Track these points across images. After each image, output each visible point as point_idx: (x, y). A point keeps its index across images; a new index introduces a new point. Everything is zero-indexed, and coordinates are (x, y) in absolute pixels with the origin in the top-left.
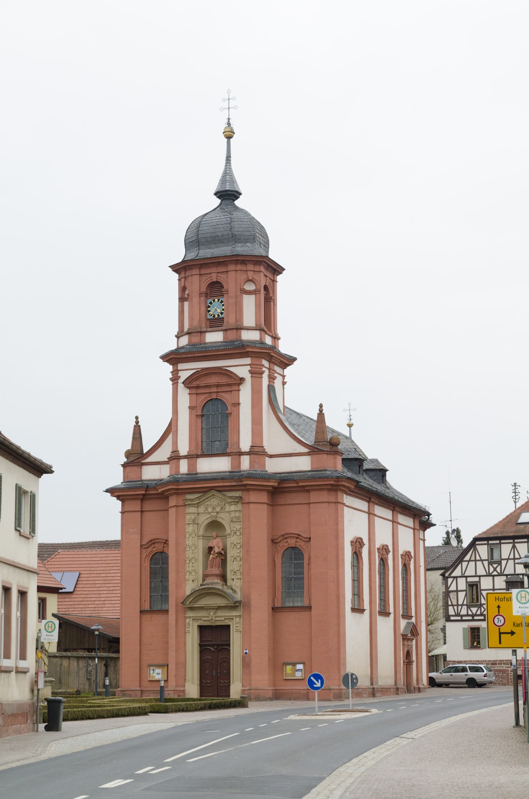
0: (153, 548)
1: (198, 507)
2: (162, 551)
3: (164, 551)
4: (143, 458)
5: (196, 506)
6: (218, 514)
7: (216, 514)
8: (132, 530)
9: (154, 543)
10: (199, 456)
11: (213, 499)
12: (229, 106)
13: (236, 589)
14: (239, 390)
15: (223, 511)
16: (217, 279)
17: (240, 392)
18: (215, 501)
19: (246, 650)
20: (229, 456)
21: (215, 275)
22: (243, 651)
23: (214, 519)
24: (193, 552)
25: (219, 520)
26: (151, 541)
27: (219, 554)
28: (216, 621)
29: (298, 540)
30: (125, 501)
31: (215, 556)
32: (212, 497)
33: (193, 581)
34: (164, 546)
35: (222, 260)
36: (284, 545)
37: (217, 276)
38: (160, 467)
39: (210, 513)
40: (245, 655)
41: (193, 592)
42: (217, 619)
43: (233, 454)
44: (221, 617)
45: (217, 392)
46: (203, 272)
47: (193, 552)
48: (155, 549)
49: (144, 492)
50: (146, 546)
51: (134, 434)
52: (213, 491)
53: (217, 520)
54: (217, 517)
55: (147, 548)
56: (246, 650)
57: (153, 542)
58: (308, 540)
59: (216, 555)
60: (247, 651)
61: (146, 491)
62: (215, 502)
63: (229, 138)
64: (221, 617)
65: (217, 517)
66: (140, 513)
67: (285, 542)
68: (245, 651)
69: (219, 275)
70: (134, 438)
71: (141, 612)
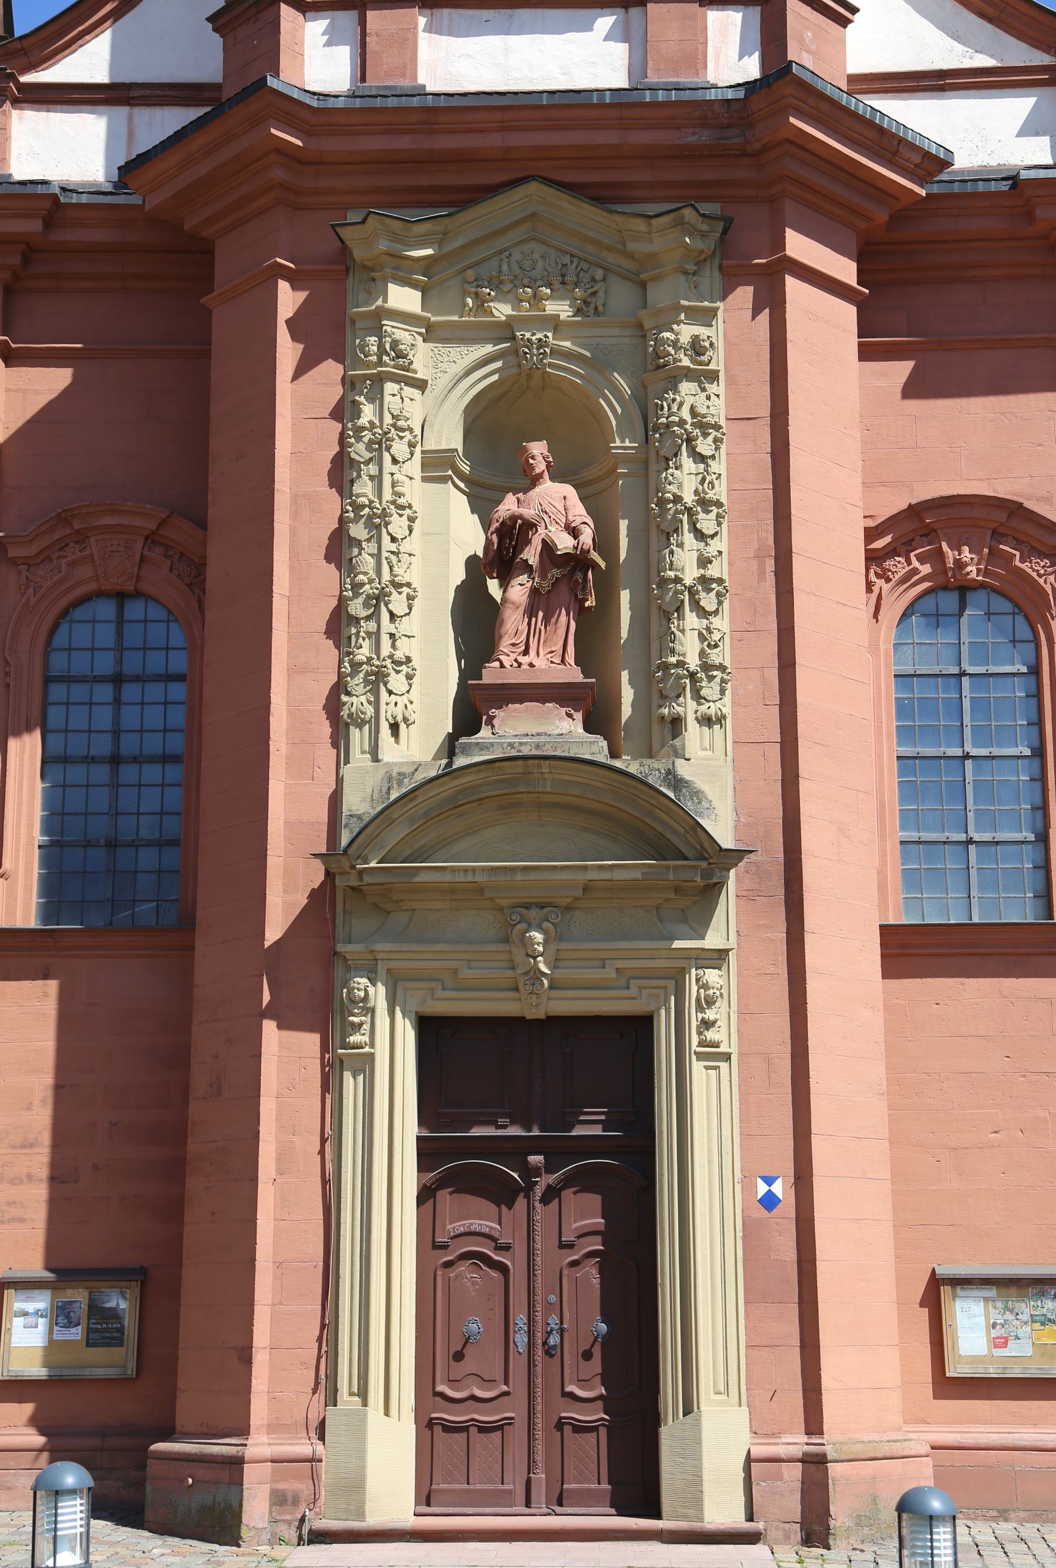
0: (72, 564)
2: (129, 587)
9: (81, 538)
11: (527, 248)
13: (699, 783)
18: (536, 256)
19: (769, 1181)
22: (748, 1188)
24: (393, 547)
26: (63, 519)
33: (395, 728)
34: (142, 559)
36: (915, 571)
38: (130, 118)
40: (761, 1212)
41: (394, 795)
47: (393, 547)
48: (85, 571)
52: (533, 188)
56: (769, 1181)
57: (77, 525)
59: (556, 573)
60: (777, 1188)
68: (762, 1188)
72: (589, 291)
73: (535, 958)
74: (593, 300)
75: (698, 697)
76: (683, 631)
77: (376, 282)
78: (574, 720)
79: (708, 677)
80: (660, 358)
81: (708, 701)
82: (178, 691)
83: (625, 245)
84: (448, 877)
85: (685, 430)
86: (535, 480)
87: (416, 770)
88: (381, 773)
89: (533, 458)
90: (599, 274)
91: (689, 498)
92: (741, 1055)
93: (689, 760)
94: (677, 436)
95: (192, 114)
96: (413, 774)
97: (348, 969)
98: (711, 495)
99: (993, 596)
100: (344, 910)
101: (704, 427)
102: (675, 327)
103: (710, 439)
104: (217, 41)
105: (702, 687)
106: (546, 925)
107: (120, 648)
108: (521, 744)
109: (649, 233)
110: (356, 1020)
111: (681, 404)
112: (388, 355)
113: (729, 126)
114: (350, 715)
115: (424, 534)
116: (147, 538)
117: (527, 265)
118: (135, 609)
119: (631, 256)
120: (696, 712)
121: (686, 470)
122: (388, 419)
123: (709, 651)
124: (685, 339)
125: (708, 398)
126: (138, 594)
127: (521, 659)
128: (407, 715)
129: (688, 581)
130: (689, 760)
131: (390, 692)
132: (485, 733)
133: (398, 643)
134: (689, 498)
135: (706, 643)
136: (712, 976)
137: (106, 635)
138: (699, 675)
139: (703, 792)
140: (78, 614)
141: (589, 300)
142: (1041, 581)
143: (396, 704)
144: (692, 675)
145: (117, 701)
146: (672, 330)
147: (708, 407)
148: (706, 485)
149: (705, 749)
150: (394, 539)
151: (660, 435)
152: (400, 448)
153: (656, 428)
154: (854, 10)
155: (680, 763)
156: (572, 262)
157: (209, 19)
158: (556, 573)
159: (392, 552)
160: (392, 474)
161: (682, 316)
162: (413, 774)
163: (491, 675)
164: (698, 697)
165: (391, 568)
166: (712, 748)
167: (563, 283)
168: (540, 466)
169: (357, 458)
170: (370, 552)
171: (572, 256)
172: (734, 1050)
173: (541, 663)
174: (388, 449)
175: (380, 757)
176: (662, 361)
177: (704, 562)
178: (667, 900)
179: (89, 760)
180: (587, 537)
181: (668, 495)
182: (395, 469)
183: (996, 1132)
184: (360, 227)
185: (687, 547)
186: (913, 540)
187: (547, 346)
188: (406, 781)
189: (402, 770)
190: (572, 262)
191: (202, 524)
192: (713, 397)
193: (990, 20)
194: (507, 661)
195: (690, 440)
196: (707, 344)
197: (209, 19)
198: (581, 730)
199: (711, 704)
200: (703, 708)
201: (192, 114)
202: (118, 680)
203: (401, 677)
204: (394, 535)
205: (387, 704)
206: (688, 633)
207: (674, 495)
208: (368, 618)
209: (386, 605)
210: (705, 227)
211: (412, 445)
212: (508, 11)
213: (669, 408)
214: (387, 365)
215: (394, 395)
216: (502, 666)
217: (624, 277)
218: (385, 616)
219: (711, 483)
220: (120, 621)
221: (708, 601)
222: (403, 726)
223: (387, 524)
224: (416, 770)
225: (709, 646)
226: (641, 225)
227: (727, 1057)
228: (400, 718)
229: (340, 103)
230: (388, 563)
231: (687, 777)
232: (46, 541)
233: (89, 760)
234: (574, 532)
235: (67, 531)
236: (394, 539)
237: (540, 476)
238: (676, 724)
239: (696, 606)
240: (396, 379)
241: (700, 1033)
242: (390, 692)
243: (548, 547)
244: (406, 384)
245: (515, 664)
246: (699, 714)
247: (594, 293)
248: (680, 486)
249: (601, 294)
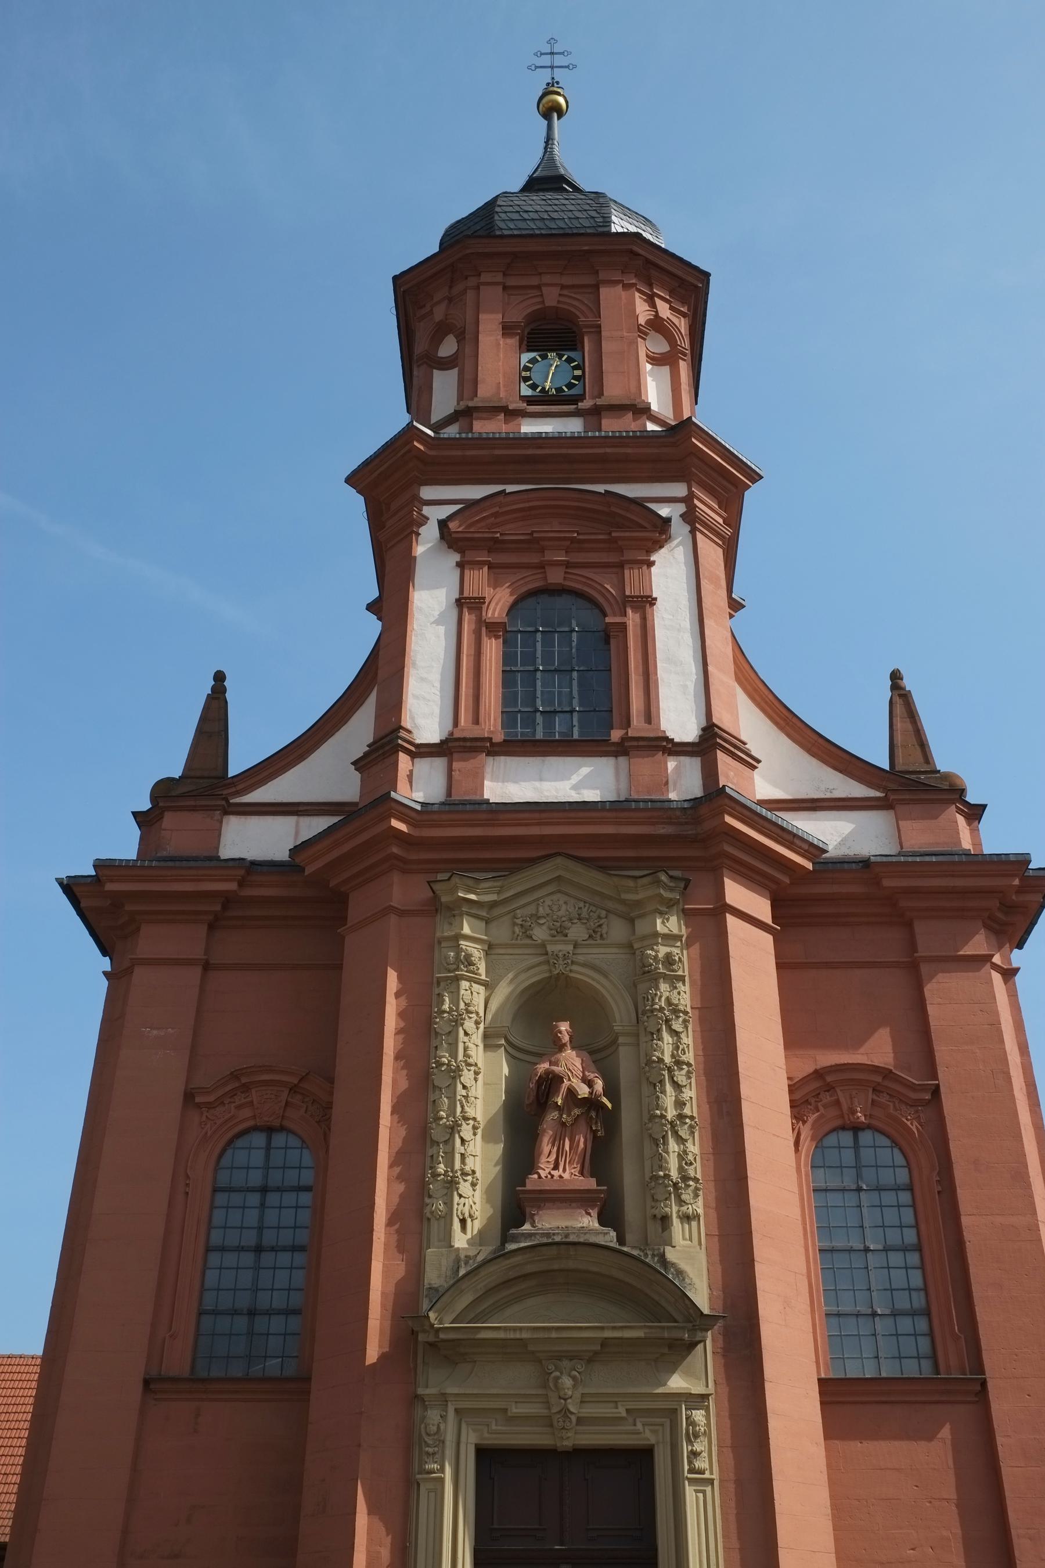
0: (239, 1107)
1: (487, 922)
2: (276, 1123)
3: (286, 1123)
4: (233, 790)
5: (484, 914)
6: (579, 951)
7: (570, 948)
8: (155, 1032)
9: (246, 1088)
10: (496, 749)
11: (555, 897)
12: (556, 53)
13: (683, 1265)
14: (651, 564)
15: (599, 942)
16: (559, 302)
17: (654, 570)
18: (561, 902)
20: (616, 754)
21: (556, 291)
23: (560, 968)
24: (464, 1093)
25: (580, 973)
26: (235, 1076)
27: (589, 1110)
28: (580, 1421)
29: (883, 1099)
30: (138, 929)
31: (569, 1115)
32: (550, 889)
33: (463, 1222)
34: (287, 1103)
35: (586, 248)
37: (560, 295)
38: (297, 824)
39: (543, 945)
41: (462, 1272)
42: (588, 1411)
43: (641, 743)
44: (613, 1399)
45: (568, 565)
46: (512, 282)
47: (464, 1093)
48: (247, 1113)
49: (233, 886)
50: (211, 1098)
51: (204, 719)
52: (559, 860)
53: (572, 975)
54: (573, 962)
55: (209, 1106)
57: (244, 1080)
58: (928, 1097)
61: (241, 884)
62: (564, 907)
63: (550, 111)
64: (613, 1399)
65: (573, 962)
66: (199, 970)
67: (825, 1101)
69: (565, 292)
70: (200, 732)
71: (147, 1382)
72: (597, 924)
73: (565, 1400)
74: (600, 930)
75: (681, 1202)
76: (667, 1153)
77: (456, 918)
78: (591, 1216)
79: (685, 1185)
80: (645, 967)
81: (688, 1204)
82: (305, 1198)
83: (620, 896)
84: (501, 1335)
85: (665, 1014)
86: (561, 1047)
87: (478, 1253)
88: (453, 1256)
89: (560, 1032)
90: (603, 913)
91: (668, 1059)
92: (721, 1481)
93: (674, 1247)
94: (659, 1018)
95: (335, 819)
96: (476, 1256)
97: (426, 1409)
98: (684, 1058)
99: (877, 1135)
100: (423, 1361)
101: (676, 1011)
102: (655, 947)
103: (681, 1019)
104: (357, 776)
105: (682, 1193)
106: (574, 1373)
107: (267, 1167)
108: (554, 1234)
109: (636, 887)
110: (430, 1450)
111: (661, 997)
112: (463, 964)
113: (686, 823)
114: (432, 1213)
115: (485, 1084)
116: (291, 1089)
117: (555, 908)
118: (279, 1139)
119: (623, 902)
120: (679, 1211)
121: (666, 1042)
122: (462, 1006)
123: (686, 1167)
124: (661, 955)
125: (679, 993)
126: (282, 1129)
127: (553, 1172)
128: (472, 1213)
129: (669, 1118)
130: (674, 1247)
131: (460, 1196)
132: (527, 1227)
133: (467, 1160)
135: (684, 1162)
136: (699, 1415)
137: (257, 1158)
138: (680, 1185)
139: (686, 1272)
140: (240, 1143)
141: (597, 930)
142: (909, 1123)
143: (464, 1204)
144: (675, 1185)
145: (263, 1205)
146: (652, 949)
147: (679, 999)
148: (680, 1052)
149: (686, 1240)
150: (464, 1087)
151: (648, 1017)
153: (644, 1013)
154: (758, 761)
155: (668, 1249)
156: (585, 906)
157: (352, 763)
158: (576, 1112)
159: (463, 1096)
160: (464, 1043)
161: (660, 940)
162: (476, 1256)
163: (532, 1182)
164: (681, 1202)
165: (462, 1107)
166: (691, 1239)
167: (579, 919)
168: (566, 1038)
169: (441, 1032)
170: (448, 1095)
171: (585, 902)
172: (715, 1476)
173: (566, 1176)
174: (462, 1025)
175: (452, 1244)
176: (647, 969)
177: (680, 1104)
178: (663, 1354)
179: (240, 1249)
180: (599, 1085)
181: (654, 1058)
182: (466, 1039)
183: (913, 1549)
184: (447, 882)
185: (668, 1094)
186: (819, 1094)
187: (569, 959)
188: (471, 1261)
189: (468, 1254)
190: (585, 906)
191: (331, 1080)
192: (682, 993)
193: (841, 772)
194: (543, 1174)
195: (667, 1021)
196: (677, 958)
197: (352, 763)
198: (597, 1225)
199: (690, 1206)
200: (684, 1209)
201: (335, 819)
202: (264, 1190)
203: (468, 1184)
204: (465, 1084)
205: (458, 1204)
206: (671, 1154)
207: (658, 1057)
208: (446, 1142)
209: (459, 1132)
210: (672, 884)
211: (477, 1023)
212: (542, 758)
213: (653, 1000)
214: (462, 971)
215: (466, 990)
216: (540, 1177)
217: (619, 916)
218: (458, 1141)
219: (683, 1050)
220: (268, 1148)
221: (683, 1132)
222: (469, 1221)
223: (460, 1076)
224: (478, 1253)
225: (686, 1164)
226: (631, 883)
227: (711, 1482)
228: (467, 1215)
229: (436, 808)
230: (460, 1103)
231: (674, 1261)
232: (220, 1092)
233: (240, 1249)
234: (590, 1084)
235: (237, 1085)
236: (464, 1087)
237: (565, 1045)
238: (665, 1220)
239: (676, 1134)
240: (469, 980)
241: (690, 1462)
242: (460, 1196)
243: (571, 1092)
244: (475, 983)
245: (549, 1176)
246: (680, 1213)
247: (600, 926)
248: (663, 1053)
249: (605, 926)
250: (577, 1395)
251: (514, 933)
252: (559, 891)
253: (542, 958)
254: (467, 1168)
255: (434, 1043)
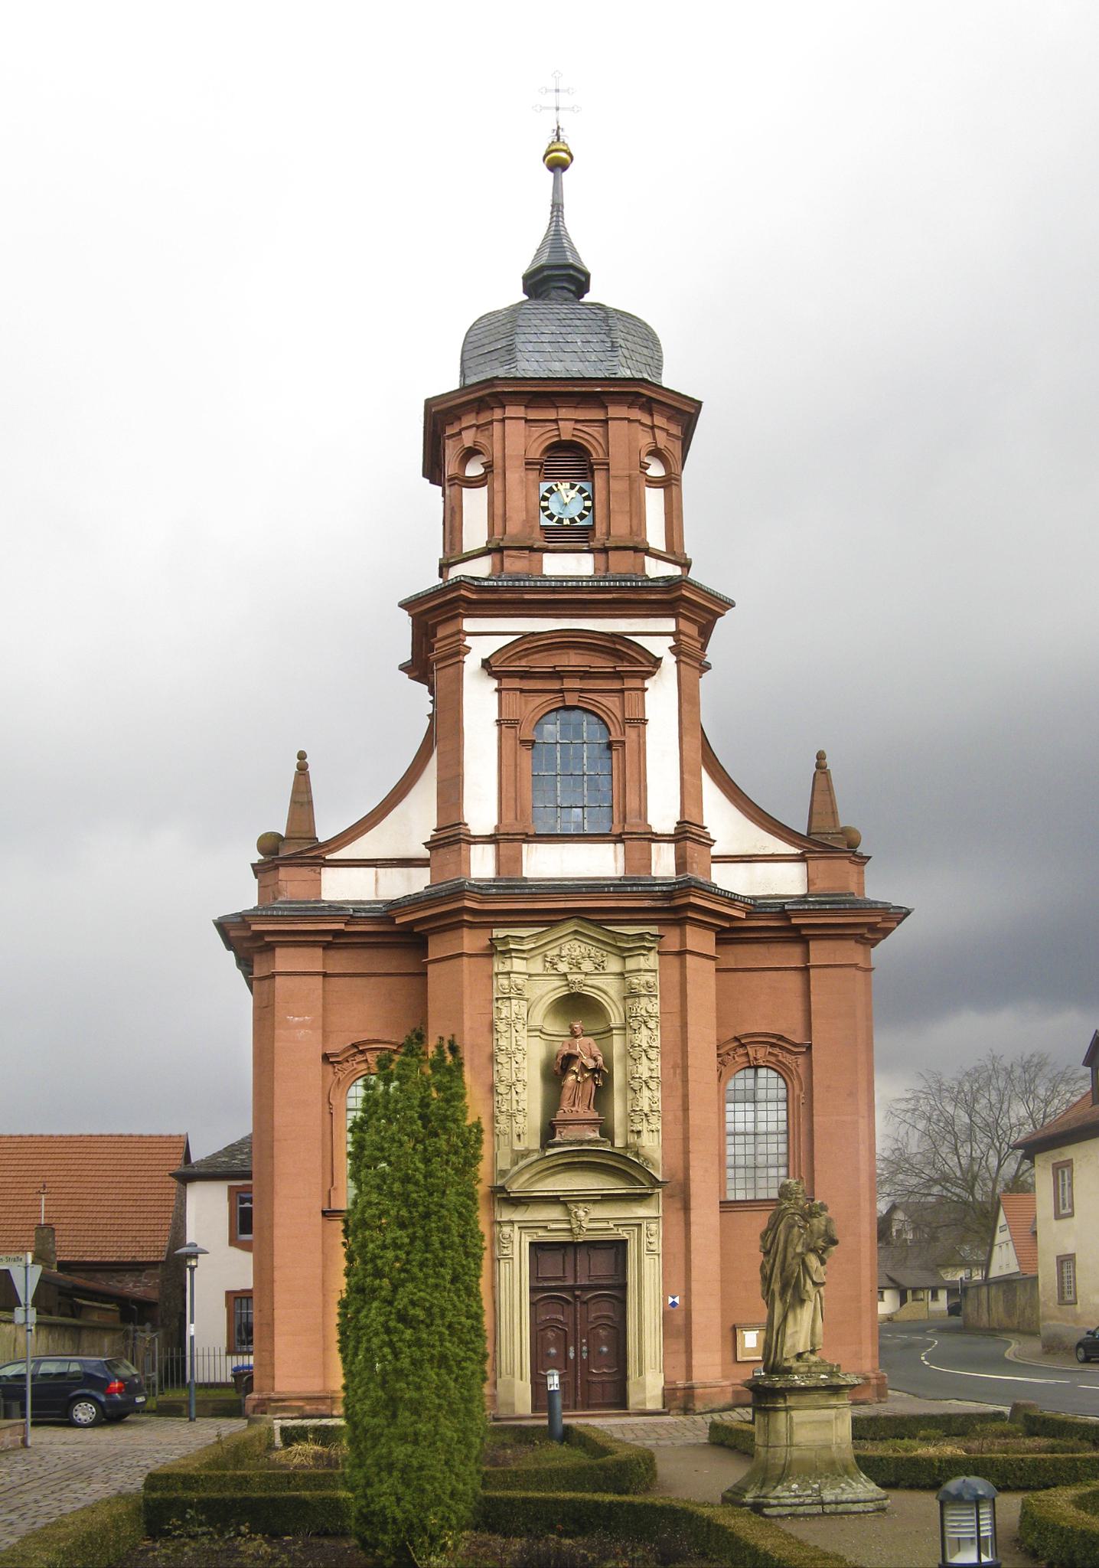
18: (576, 946)
24: (517, 1066)
33: (519, 1136)
39: (565, 975)
47: (517, 1066)
91: (645, 1045)
97: (501, 1227)
117: (572, 950)
134: (645, 1045)
152: (519, 1027)
163: (560, 1115)
203: (521, 1117)
208: (507, 1094)
222: (522, 1136)
234: (595, 1059)
243: (584, 1067)
250: (587, 1219)
251: (545, 966)
252: (576, 939)
253: (565, 983)
254: (520, 1108)
255: (496, 1036)
